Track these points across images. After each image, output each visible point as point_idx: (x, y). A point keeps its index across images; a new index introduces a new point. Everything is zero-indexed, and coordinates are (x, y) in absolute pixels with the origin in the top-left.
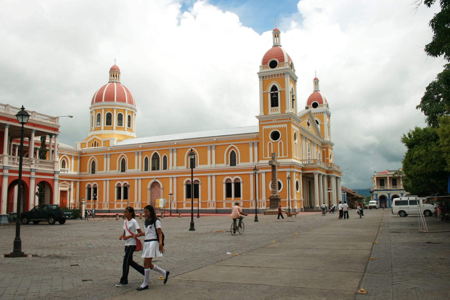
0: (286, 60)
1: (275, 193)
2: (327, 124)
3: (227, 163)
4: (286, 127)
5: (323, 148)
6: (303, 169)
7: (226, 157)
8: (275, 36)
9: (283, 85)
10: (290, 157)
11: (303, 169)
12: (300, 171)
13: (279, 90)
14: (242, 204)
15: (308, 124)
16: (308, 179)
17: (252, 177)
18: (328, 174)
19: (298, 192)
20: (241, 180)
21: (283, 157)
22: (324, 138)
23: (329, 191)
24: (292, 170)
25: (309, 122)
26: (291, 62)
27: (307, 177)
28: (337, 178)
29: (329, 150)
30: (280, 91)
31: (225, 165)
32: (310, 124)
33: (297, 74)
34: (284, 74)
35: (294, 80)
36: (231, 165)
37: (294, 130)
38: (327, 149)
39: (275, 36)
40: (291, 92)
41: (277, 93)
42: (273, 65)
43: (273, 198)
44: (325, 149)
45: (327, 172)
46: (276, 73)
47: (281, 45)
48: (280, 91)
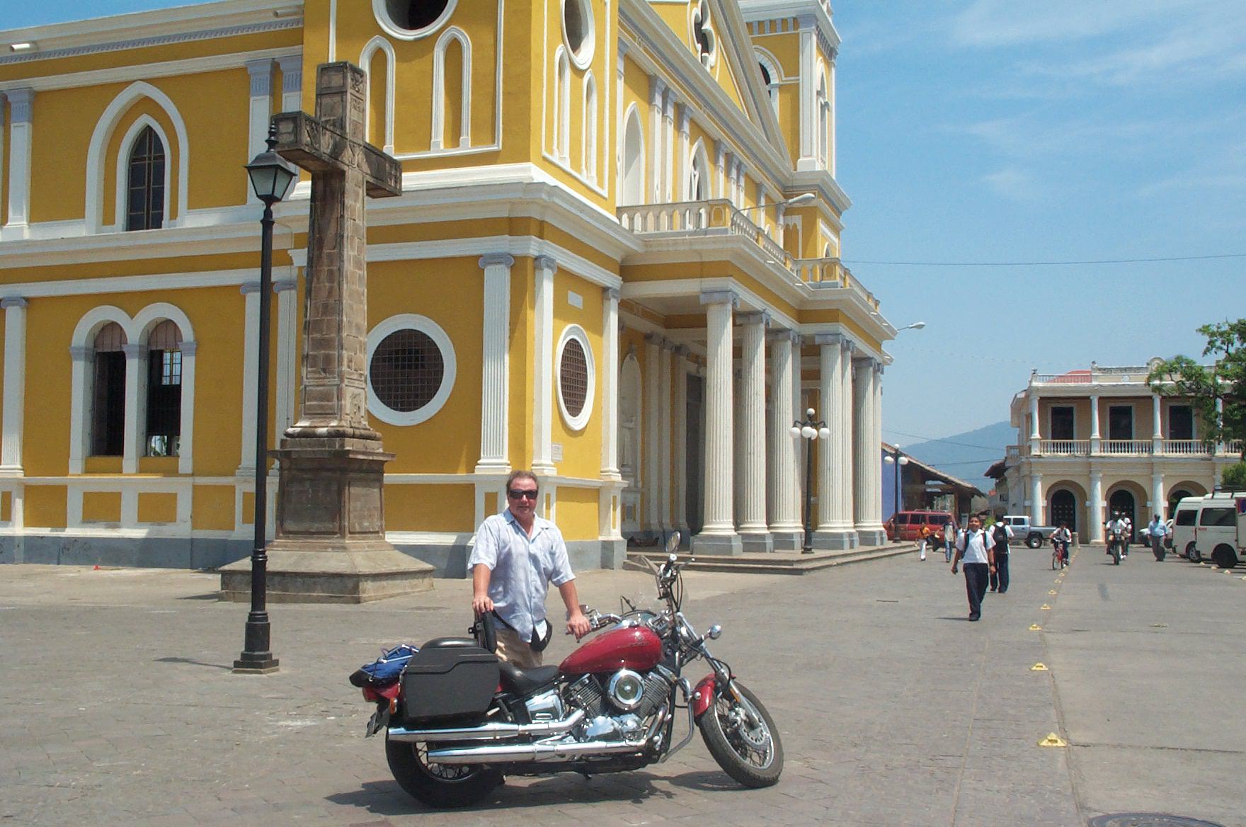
1: (326, 414)
2: (816, 86)
3: (108, 219)
5: (789, 211)
6: (628, 271)
7: (102, 171)
10: (518, 151)
11: (628, 271)
12: (611, 280)
14: (184, 508)
15: (703, 39)
16: (665, 346)
17: (253, 302)
18: (810, 329)
19: (577, 423)
20: (187, 332)
21: (466, 147)
22: (796, 155)
23: (810, 431)
24: (533, 246)
25: (707, 26)
27: (678, 349)
28: (860, 364)
29: (822, 226)
31: (90, 230)
32: (716, 42)
36: (134, 223)
38: (810, 214)
43: (305, 448)
44: (797, 220)
45: (803, 315)
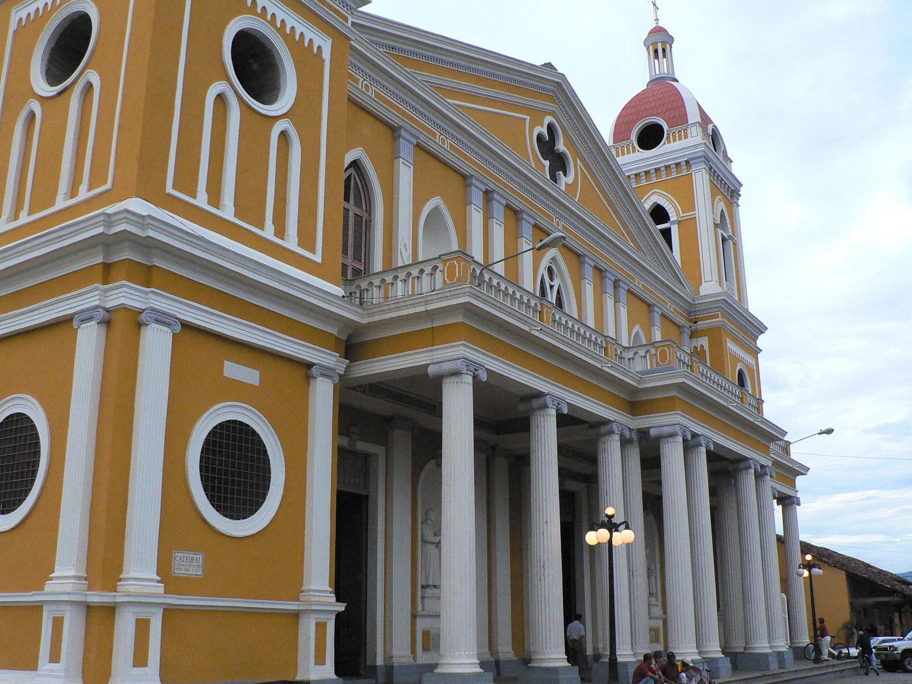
0: (693, 116)
4: (706, 348)
8: (656, 51)
9: (689, 203)
13: (673, 217)
26: (710, 127)
30: (679, 223)
33: (737, 169)
34: (687, 162)
35: (728, 190)
37: (736, 359)
39: (656, 51)
40: (716, 225)
41: (669, 230)
42: (650, 137)
46: (660, 163)
47: (676, 77)
48: (679, 223)
